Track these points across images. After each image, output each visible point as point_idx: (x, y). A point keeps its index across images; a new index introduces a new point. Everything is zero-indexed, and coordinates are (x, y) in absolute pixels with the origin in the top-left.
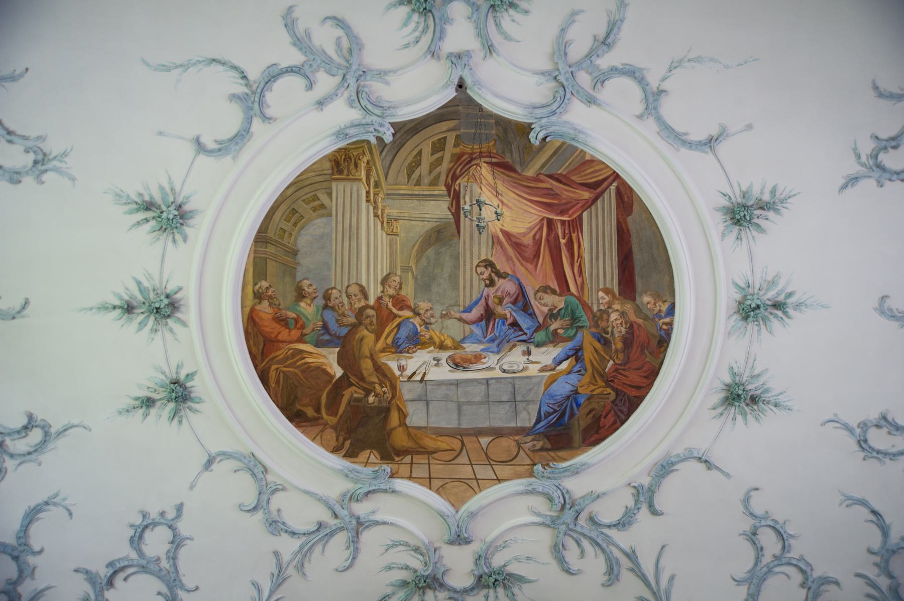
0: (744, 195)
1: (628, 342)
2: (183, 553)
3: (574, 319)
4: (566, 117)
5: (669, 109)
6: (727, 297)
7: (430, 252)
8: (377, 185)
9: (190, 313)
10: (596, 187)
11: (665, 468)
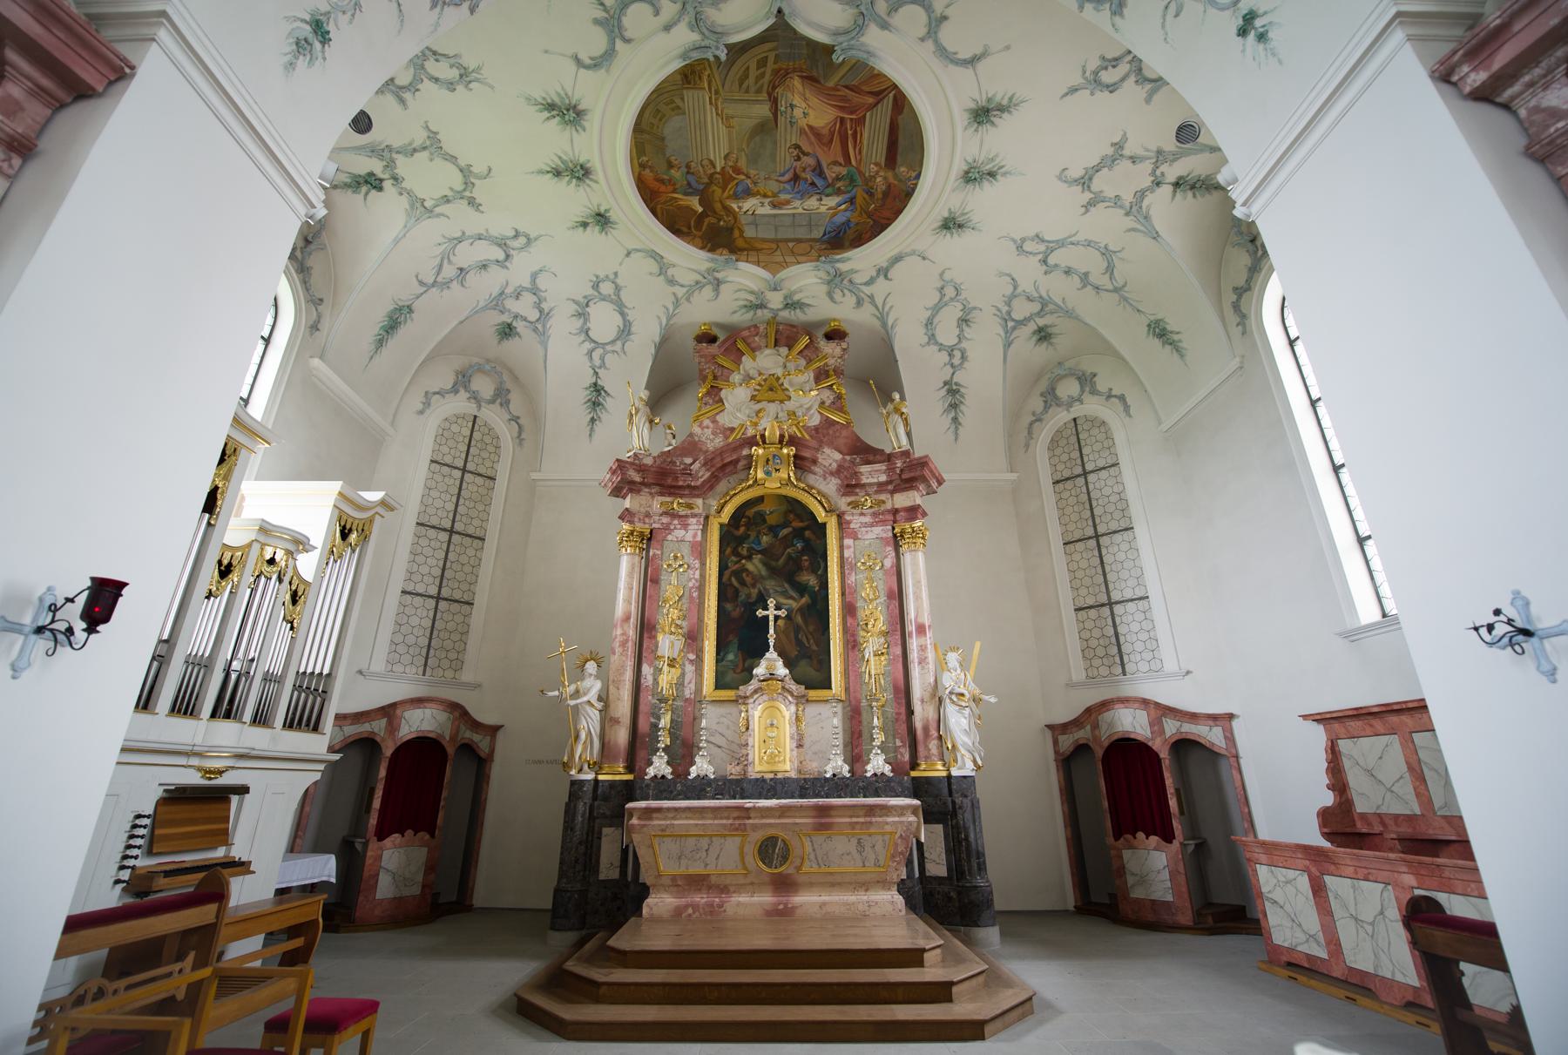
0: (989, 100)
1: (886, 194)
2: (622, 294)
3: (852, 180)
4: (862, 39)
5: (947, 35)
6: (959, 167)
7: (757, 139)
8: (717, 92)
9: (599, 174)
10: (879, 95)
11: (898, 259)
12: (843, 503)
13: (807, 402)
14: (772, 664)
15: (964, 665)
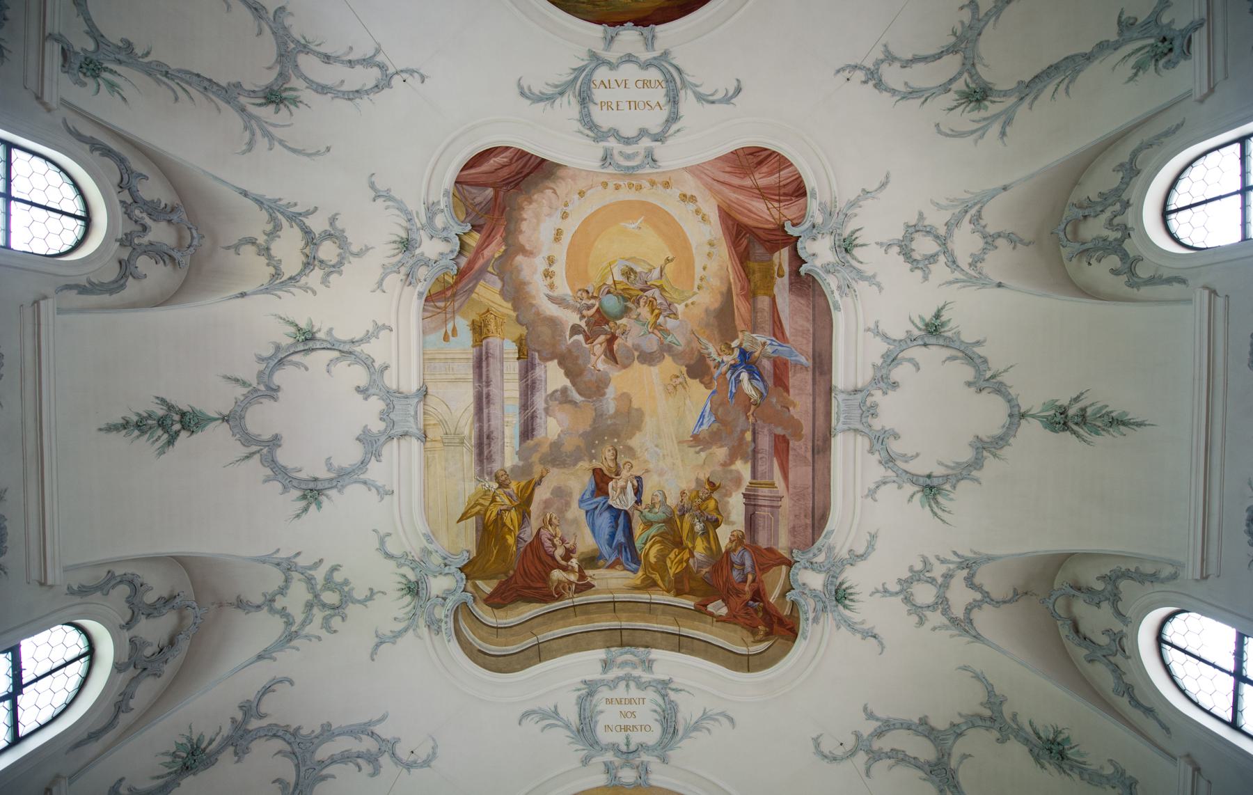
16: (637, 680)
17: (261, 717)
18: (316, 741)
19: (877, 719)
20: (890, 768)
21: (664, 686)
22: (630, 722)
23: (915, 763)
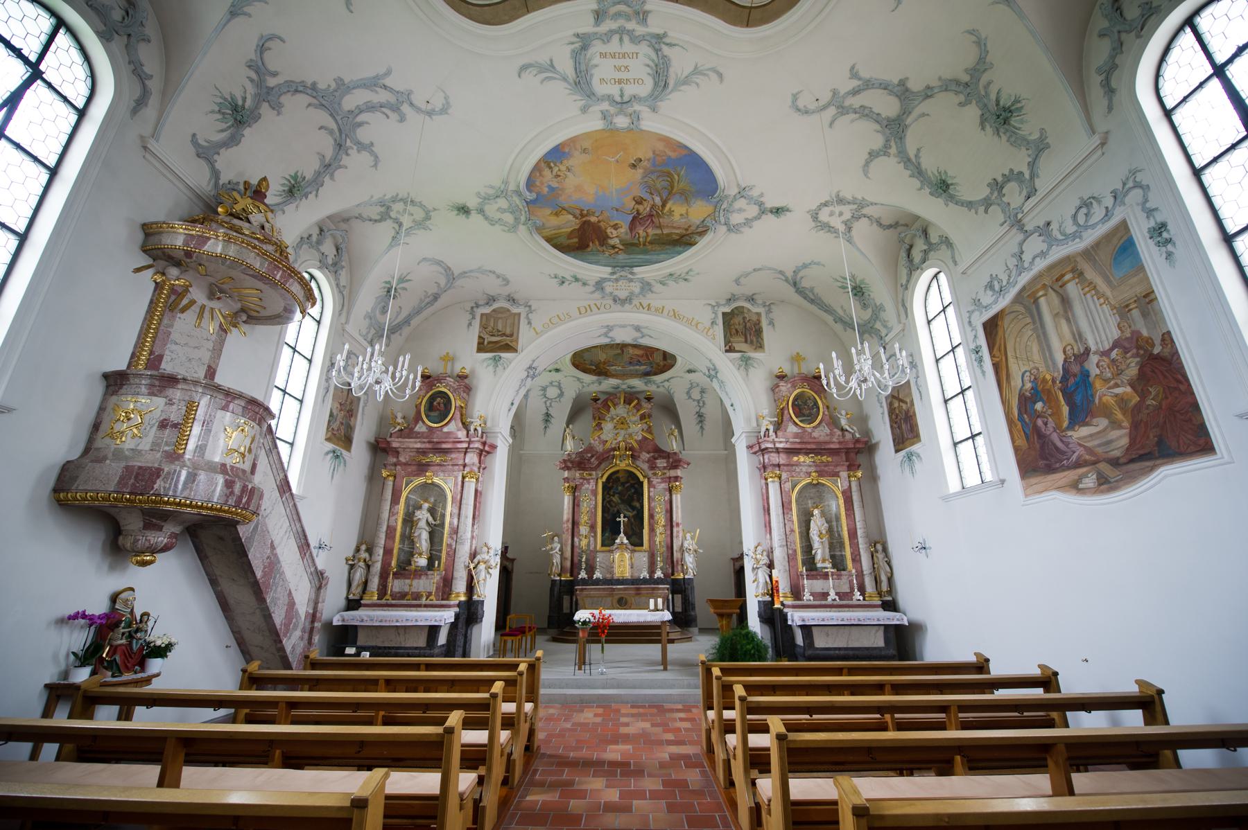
12: (650, 473)
13: (637, 430)
14: (622, 539)
15: (692, 538)
16: (630, 33)
17: (275, 74)
18: (337, 94)
19: (860, 79)
20: (852, 121)
21: (658, 40)
22: (623, 75)
23: (877, 118)
